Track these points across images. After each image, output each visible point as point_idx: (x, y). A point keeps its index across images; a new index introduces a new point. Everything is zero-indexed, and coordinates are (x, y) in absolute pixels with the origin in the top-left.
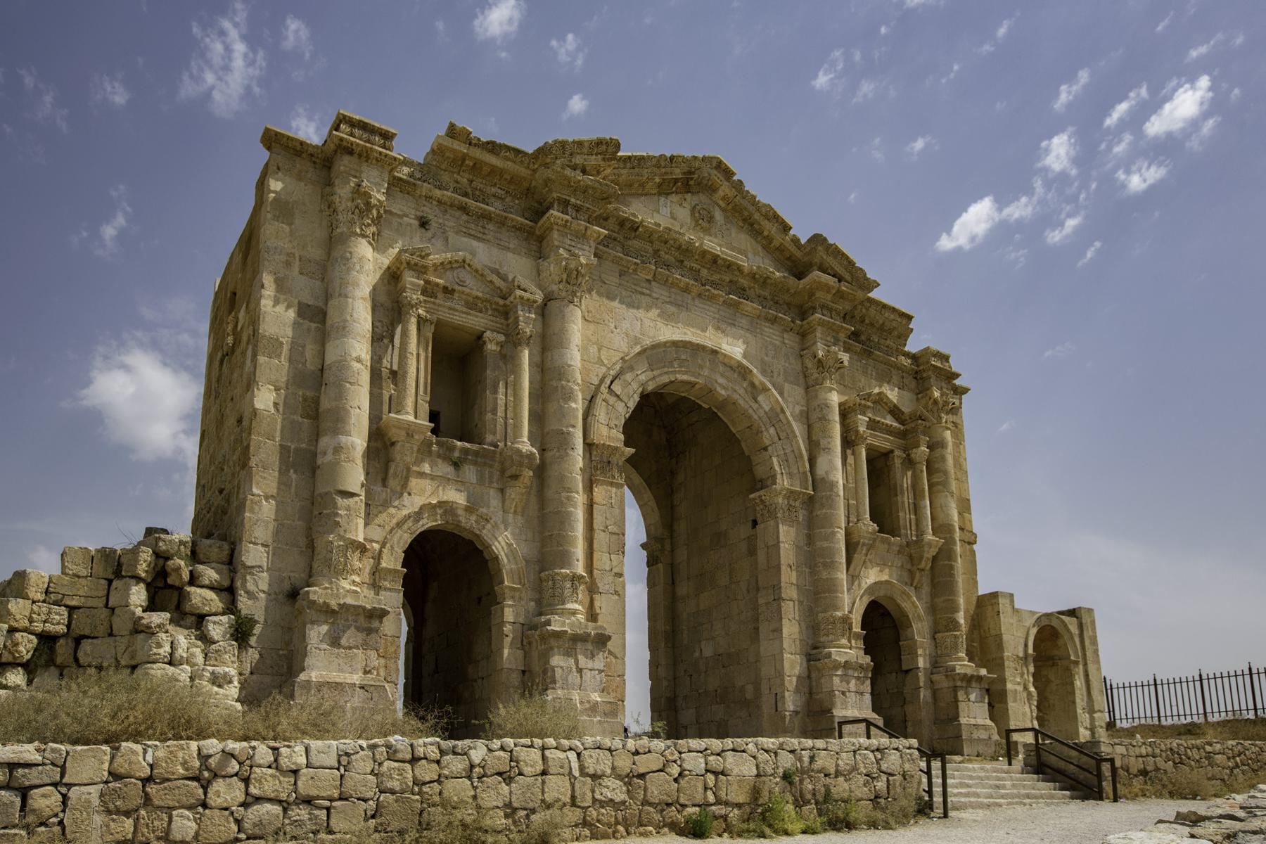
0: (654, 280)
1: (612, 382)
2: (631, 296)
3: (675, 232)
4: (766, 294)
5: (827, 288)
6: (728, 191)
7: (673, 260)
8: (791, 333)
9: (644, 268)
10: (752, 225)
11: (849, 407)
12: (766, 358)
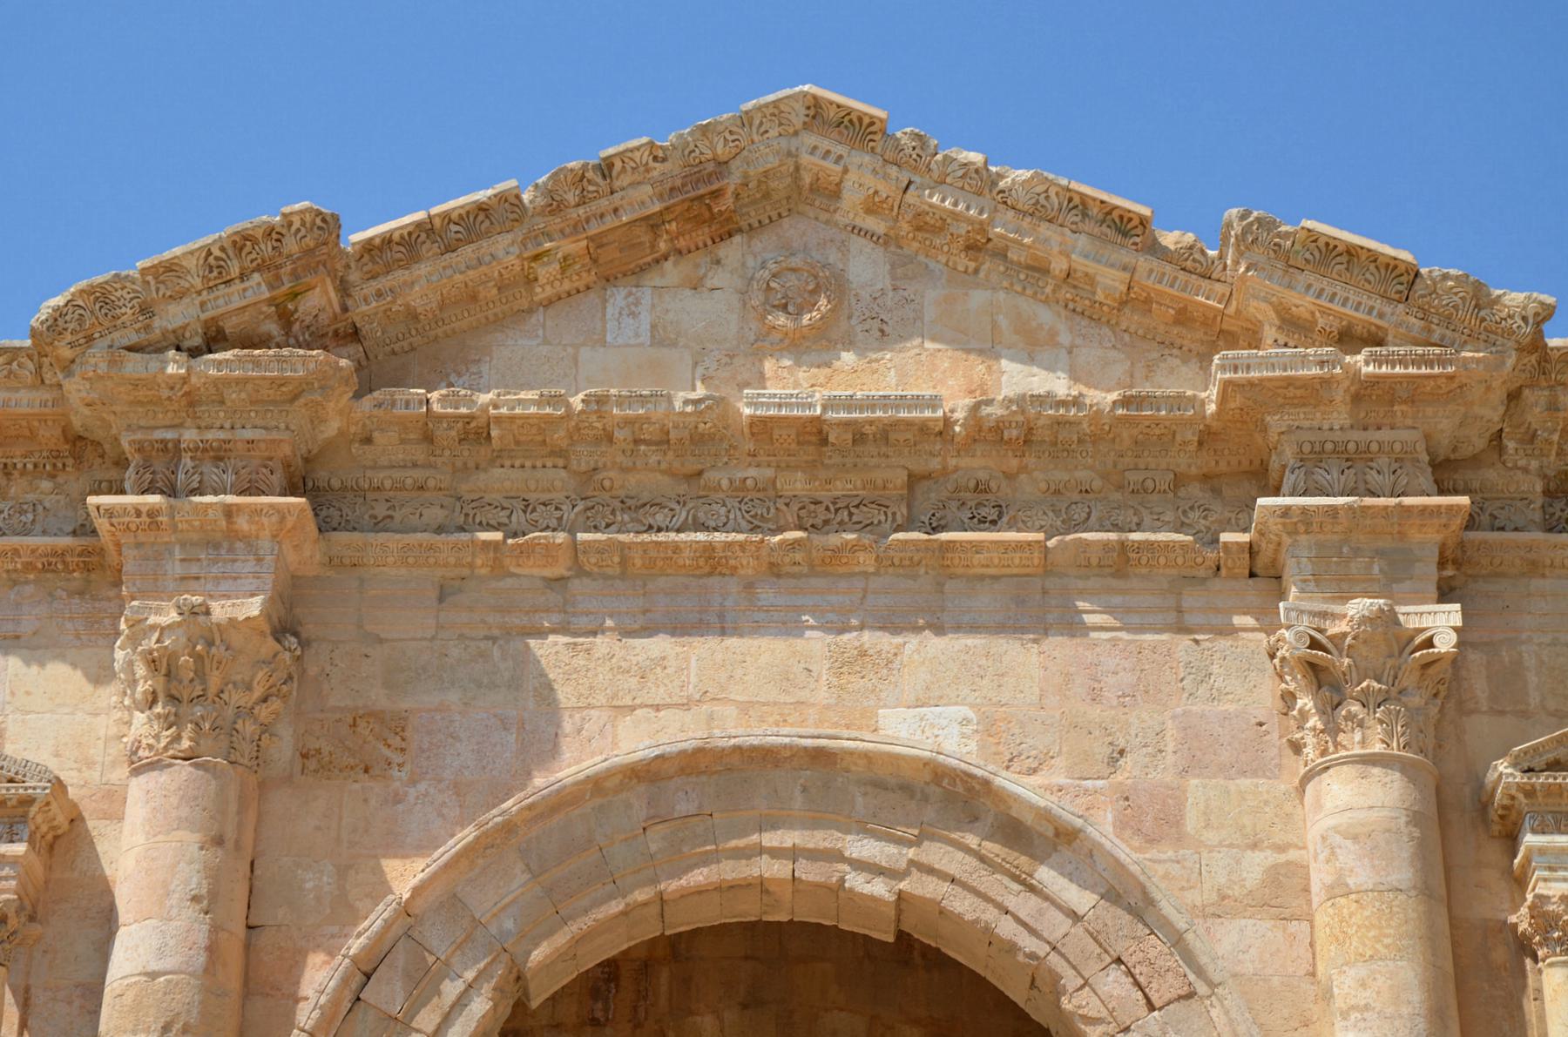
0: (580, 572)
1: (368, 976)
2: (483, 655)
3: (621, 401)
4: (1081, 474)
5: (1312, 393)
6: (871, 182)
7: (666, 480)
8: (1217, 584)
9: (526, 551)
10: (1002, 254)
11: (1504, 807)
12: (1095, 712)
